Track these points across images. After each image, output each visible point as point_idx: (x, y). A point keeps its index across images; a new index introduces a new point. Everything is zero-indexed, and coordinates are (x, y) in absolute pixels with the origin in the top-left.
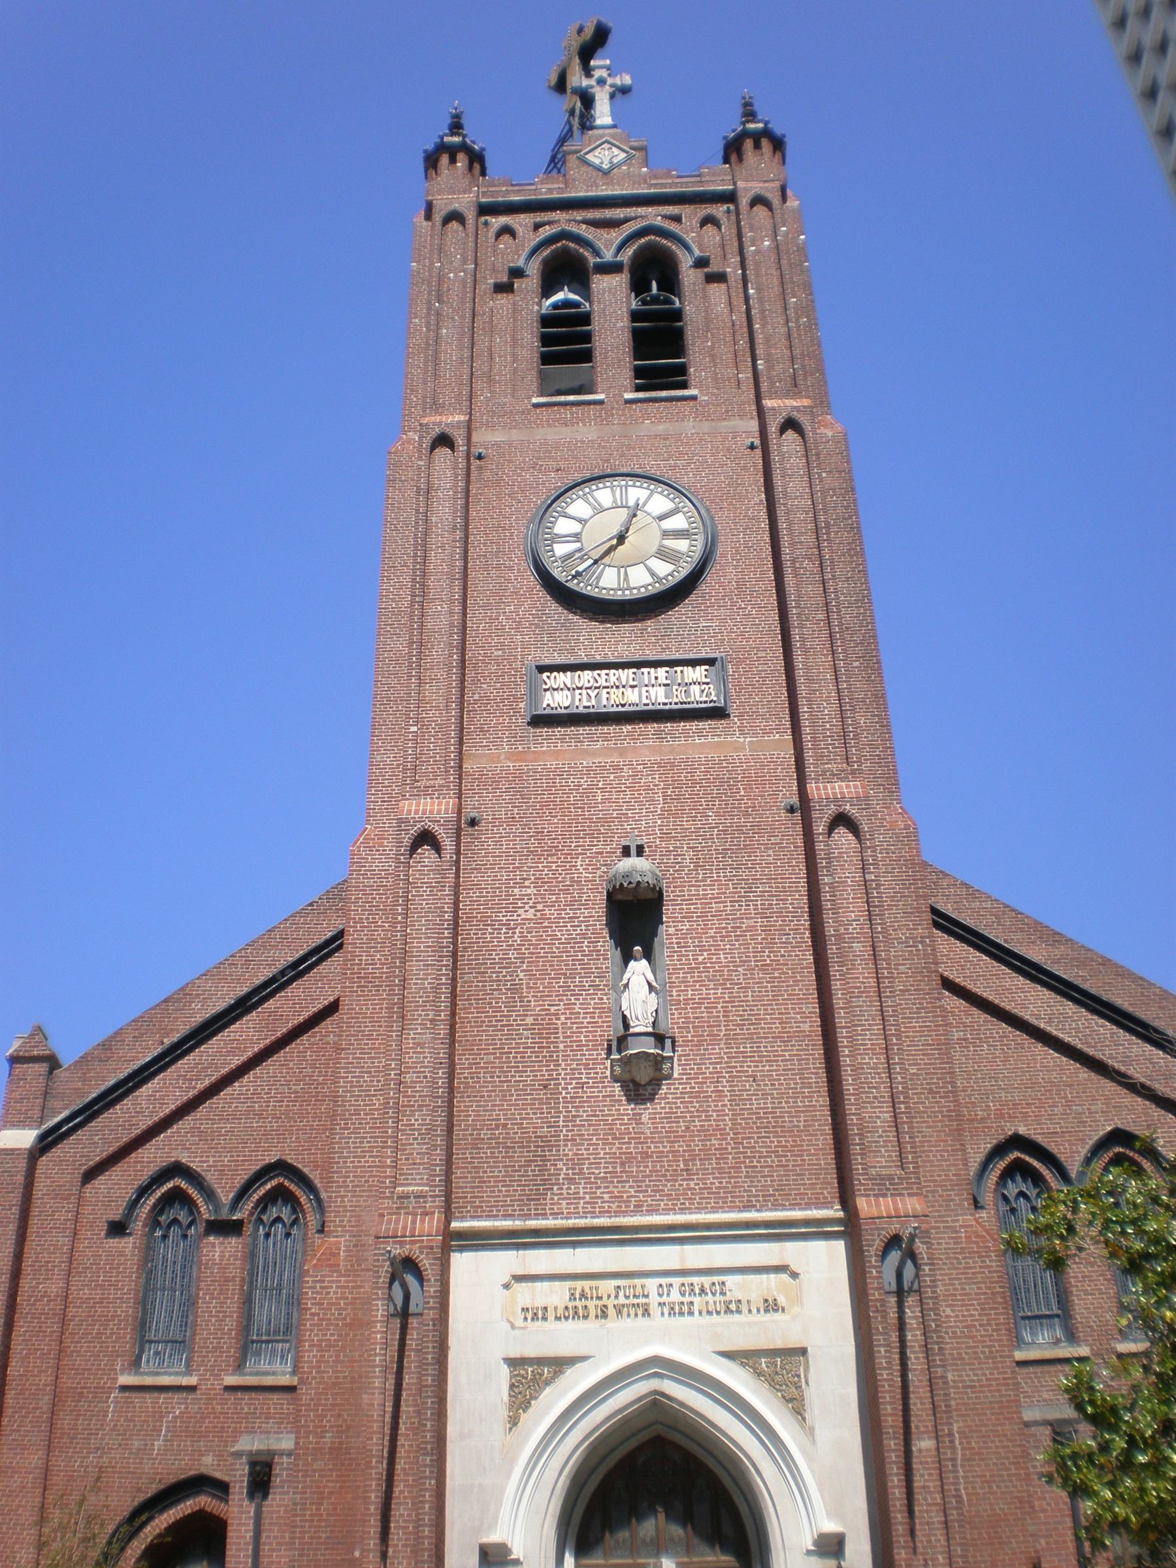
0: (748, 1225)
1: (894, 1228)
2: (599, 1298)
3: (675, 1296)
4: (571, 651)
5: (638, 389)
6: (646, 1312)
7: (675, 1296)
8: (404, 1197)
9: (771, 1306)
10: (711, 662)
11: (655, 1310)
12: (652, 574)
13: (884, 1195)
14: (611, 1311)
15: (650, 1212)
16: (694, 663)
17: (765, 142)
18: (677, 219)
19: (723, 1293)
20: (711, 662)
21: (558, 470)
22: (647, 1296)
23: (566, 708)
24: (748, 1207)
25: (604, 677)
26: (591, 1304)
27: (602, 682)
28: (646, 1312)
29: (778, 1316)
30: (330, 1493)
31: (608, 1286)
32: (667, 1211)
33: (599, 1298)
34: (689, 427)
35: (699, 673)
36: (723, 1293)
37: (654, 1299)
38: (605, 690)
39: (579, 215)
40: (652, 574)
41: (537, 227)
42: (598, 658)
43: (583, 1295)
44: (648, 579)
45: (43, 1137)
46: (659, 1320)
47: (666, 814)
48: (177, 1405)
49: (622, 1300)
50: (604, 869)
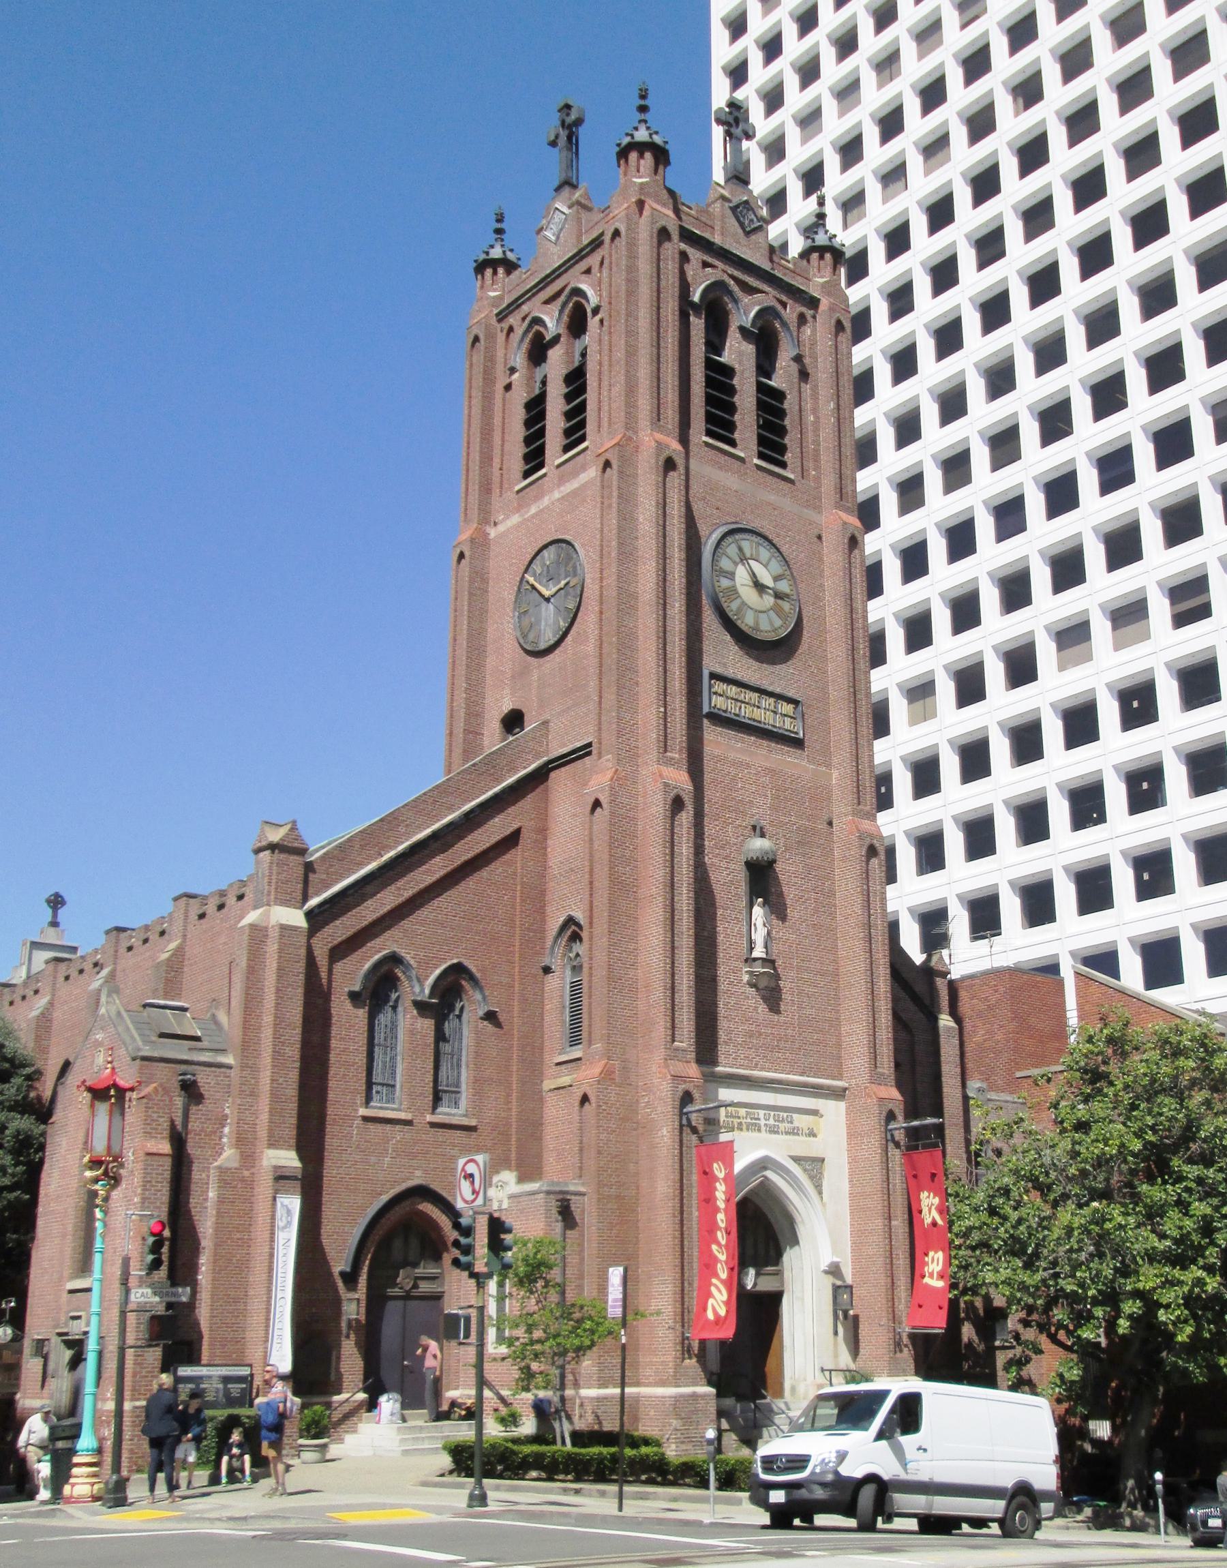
0: (805, 1085)
1: (890, 1106)
2: (739, 1118)
3: (771, 1122)
4: (725, 665)
5: (761, 456)
6: (759, 1130)
7: (771, 1122)
8: (677, 1049)
9: (812, 1134)
10: (795, 702)
11: (763, 1128)
12: (771, 624)
13: (880, 1084)
14: (744, 1127)
15: (762, 1069)
16: (790, 701)
17: (828, 256)
18: (784, 305)
19: (792, 1122)
20: (795, 702)
21: (717, 509)
22: (759, 1119)
23: (725, 711)
24: (802, 1074)
25: (743, 695)
26: (736, 1121)
27: (742, 697)
28: (759, 1130)
29: (812, 1139)
30: (617, 1224)
31: (742, 1111)
32: (769, 1070)
33: (739, 1118)
34: (786, 503)
35: (787, 708)
36: (792, 1122)
37: (762, 1122)
38: (743, 705)
39: (731, 270)
40: (771, 624)
41: (706, 265)
42: (739, 677)
43: (732, 1116)
44: (769, 628)
45: (309, 915)
46: (764, 1135)
47: (772, 808)
48: (398, 1133)
49: (749, 1120)
50: (742, 838)
